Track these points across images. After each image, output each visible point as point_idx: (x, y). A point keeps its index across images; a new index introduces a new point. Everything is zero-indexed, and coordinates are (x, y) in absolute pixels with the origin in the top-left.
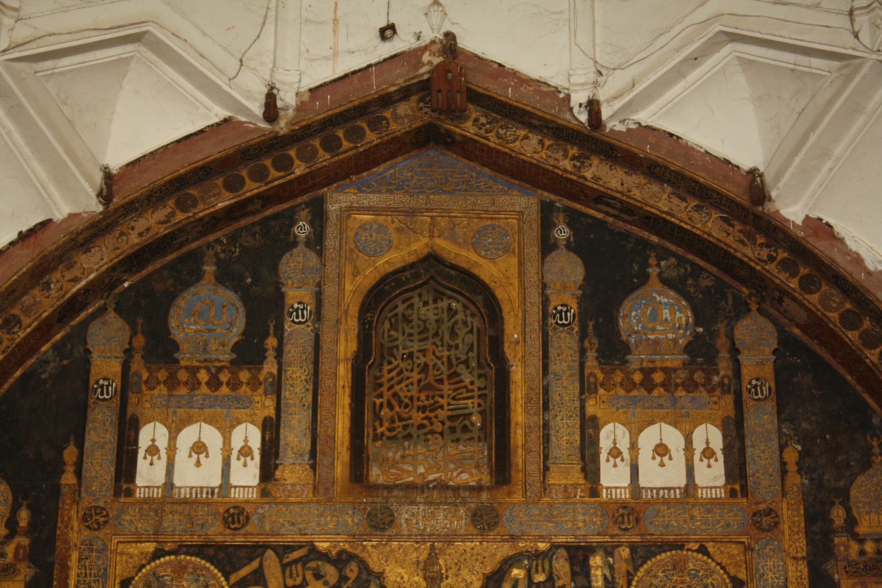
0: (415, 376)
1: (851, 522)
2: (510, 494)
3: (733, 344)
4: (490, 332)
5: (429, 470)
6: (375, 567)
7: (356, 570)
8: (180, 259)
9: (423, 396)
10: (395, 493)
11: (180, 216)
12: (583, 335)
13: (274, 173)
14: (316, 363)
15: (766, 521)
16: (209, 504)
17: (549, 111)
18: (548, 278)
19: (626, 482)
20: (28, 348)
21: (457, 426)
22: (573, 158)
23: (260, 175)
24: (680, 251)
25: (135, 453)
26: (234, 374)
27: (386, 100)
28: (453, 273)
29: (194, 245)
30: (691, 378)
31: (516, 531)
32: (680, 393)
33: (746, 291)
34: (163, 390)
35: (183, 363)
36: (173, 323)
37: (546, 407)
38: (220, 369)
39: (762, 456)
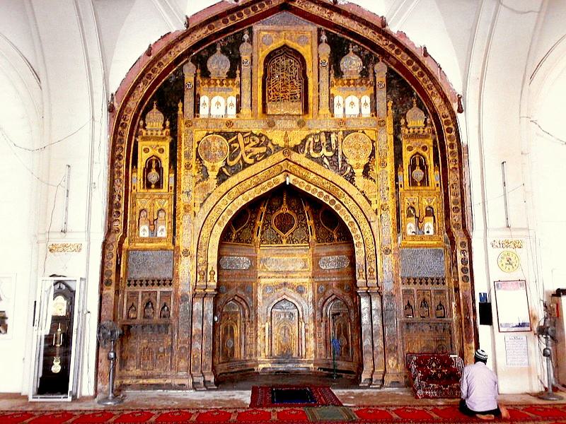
1: (406, 123)
6: (270, 137)
8: (210, 46)
11: (210, 32)
13: (237, 18)
15: (382, 123)
23: (233, 19)
24: (359, 43)
25: (199, 105)
29: (214, 41)
31: (310, 127)
32: (358, 86)
33: (378, 55)
34: (207, 86)
36: (208, 66)
37: (319, 91)
39: (381, 105)
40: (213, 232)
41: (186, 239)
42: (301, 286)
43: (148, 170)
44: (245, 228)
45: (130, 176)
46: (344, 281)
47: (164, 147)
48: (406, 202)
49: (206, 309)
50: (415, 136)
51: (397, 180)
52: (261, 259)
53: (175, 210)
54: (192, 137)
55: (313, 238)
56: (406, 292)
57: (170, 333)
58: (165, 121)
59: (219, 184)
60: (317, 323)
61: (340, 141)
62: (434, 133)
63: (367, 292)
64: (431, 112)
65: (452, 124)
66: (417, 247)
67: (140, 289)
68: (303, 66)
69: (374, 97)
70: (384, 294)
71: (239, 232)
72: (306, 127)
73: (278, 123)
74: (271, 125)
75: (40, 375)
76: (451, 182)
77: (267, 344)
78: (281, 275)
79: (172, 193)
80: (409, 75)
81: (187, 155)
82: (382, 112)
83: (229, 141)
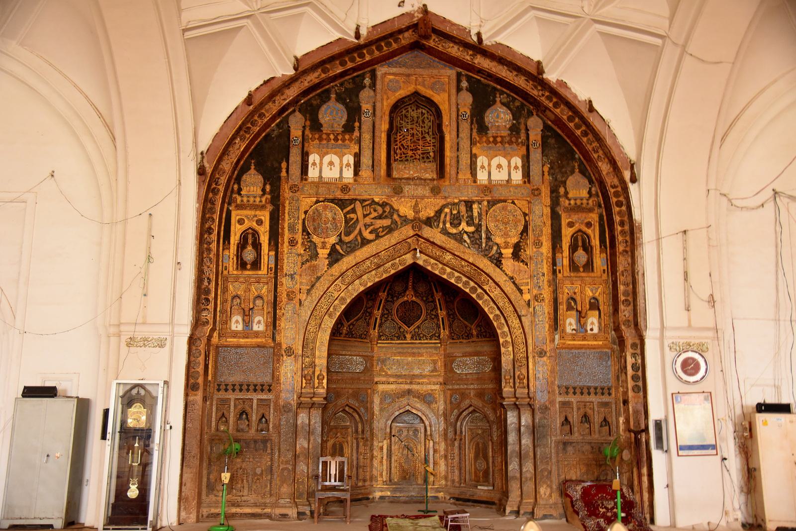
0: (409, 138)
1: (566, 193)
2: (444, 182)
3: (527, 127)
4: (437, 122)
5: (414, 172)
6: (395, 207)
7: (389, 209)
8: (322, 92)
9: (412, 146)
10: (403, 181)
11: (323, 76)
12: (472, 123)
13: (358, 59)
14: (374, 132)
15: (536, 193)
16: (335, 184)
17: (462, 36)
18: (459, 102)
19: (486, 177)
20: (267, 125)
21: (425, 157)
22: (471, 55)
23: (353, 60)
25: (308, 165)
26: (343, 136)
27: (401, 31)
28: (424, 99)
29: (327, 87)
30: (511, 140)
31: (447, 195)
32: (507, 145)
33: (532, 107)
34: (317, 142)
35: (324, 132)
36: (320, 116)
37: (458, 150)
38: (338, 134)
39: (536, 169)
40: (323, 326)
41: (289, 335)
42: (429, 394)
43: (242, 246)
44: (357, 320)
45: (221, 253)
46: (484, 389)
47: (263, 218)
48: (566, 290)
49: (313, 422)
50: (578, 209)
51: (554, 263)
52: (378, 360)
53: (275, 297)
54: (299, 205)
55: (444, 333)
56: (564, 404)
57: (269, 451)
58: (265, 185)
59: (331, 265)
60: (450, 443)
61: (484, 213)
62: (600, 206)
63: (515, 404)
64: (596, 179)
65: (622, 197)
66: (579, 348)
67: (232, 396)
68: (438, 118)
69: (526, 159)
70: (537, 406)
71: (352, 324)
72: (443, 194)
73: (406, 189)
74: (398, 191)
75: (112, 500)
76: (620, 268)
77: (385, 467)
78: (404, 380)
79: (273, 275)
80: (570, 134)
81: (292, 228)
82: (536, 178)
83: (345, 211)
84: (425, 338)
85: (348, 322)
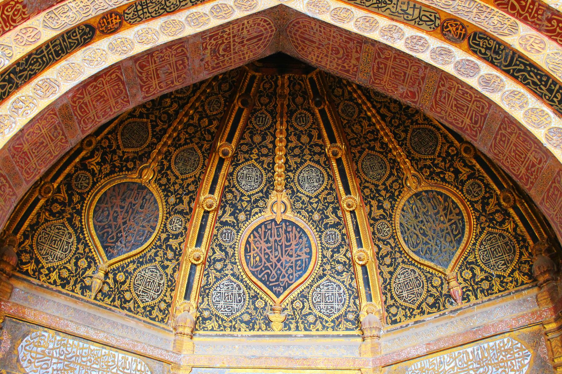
55: (372, 310)
84: (319, 326)
85: (109, 258)
